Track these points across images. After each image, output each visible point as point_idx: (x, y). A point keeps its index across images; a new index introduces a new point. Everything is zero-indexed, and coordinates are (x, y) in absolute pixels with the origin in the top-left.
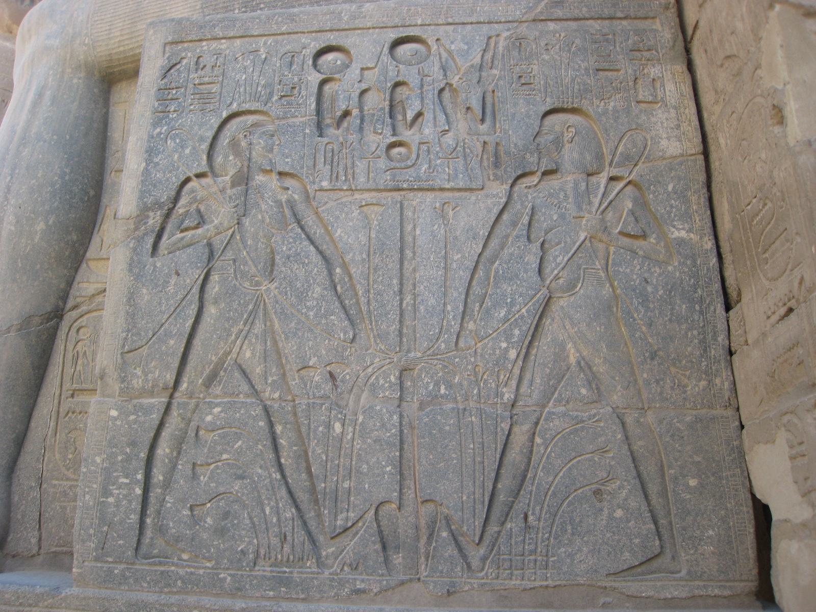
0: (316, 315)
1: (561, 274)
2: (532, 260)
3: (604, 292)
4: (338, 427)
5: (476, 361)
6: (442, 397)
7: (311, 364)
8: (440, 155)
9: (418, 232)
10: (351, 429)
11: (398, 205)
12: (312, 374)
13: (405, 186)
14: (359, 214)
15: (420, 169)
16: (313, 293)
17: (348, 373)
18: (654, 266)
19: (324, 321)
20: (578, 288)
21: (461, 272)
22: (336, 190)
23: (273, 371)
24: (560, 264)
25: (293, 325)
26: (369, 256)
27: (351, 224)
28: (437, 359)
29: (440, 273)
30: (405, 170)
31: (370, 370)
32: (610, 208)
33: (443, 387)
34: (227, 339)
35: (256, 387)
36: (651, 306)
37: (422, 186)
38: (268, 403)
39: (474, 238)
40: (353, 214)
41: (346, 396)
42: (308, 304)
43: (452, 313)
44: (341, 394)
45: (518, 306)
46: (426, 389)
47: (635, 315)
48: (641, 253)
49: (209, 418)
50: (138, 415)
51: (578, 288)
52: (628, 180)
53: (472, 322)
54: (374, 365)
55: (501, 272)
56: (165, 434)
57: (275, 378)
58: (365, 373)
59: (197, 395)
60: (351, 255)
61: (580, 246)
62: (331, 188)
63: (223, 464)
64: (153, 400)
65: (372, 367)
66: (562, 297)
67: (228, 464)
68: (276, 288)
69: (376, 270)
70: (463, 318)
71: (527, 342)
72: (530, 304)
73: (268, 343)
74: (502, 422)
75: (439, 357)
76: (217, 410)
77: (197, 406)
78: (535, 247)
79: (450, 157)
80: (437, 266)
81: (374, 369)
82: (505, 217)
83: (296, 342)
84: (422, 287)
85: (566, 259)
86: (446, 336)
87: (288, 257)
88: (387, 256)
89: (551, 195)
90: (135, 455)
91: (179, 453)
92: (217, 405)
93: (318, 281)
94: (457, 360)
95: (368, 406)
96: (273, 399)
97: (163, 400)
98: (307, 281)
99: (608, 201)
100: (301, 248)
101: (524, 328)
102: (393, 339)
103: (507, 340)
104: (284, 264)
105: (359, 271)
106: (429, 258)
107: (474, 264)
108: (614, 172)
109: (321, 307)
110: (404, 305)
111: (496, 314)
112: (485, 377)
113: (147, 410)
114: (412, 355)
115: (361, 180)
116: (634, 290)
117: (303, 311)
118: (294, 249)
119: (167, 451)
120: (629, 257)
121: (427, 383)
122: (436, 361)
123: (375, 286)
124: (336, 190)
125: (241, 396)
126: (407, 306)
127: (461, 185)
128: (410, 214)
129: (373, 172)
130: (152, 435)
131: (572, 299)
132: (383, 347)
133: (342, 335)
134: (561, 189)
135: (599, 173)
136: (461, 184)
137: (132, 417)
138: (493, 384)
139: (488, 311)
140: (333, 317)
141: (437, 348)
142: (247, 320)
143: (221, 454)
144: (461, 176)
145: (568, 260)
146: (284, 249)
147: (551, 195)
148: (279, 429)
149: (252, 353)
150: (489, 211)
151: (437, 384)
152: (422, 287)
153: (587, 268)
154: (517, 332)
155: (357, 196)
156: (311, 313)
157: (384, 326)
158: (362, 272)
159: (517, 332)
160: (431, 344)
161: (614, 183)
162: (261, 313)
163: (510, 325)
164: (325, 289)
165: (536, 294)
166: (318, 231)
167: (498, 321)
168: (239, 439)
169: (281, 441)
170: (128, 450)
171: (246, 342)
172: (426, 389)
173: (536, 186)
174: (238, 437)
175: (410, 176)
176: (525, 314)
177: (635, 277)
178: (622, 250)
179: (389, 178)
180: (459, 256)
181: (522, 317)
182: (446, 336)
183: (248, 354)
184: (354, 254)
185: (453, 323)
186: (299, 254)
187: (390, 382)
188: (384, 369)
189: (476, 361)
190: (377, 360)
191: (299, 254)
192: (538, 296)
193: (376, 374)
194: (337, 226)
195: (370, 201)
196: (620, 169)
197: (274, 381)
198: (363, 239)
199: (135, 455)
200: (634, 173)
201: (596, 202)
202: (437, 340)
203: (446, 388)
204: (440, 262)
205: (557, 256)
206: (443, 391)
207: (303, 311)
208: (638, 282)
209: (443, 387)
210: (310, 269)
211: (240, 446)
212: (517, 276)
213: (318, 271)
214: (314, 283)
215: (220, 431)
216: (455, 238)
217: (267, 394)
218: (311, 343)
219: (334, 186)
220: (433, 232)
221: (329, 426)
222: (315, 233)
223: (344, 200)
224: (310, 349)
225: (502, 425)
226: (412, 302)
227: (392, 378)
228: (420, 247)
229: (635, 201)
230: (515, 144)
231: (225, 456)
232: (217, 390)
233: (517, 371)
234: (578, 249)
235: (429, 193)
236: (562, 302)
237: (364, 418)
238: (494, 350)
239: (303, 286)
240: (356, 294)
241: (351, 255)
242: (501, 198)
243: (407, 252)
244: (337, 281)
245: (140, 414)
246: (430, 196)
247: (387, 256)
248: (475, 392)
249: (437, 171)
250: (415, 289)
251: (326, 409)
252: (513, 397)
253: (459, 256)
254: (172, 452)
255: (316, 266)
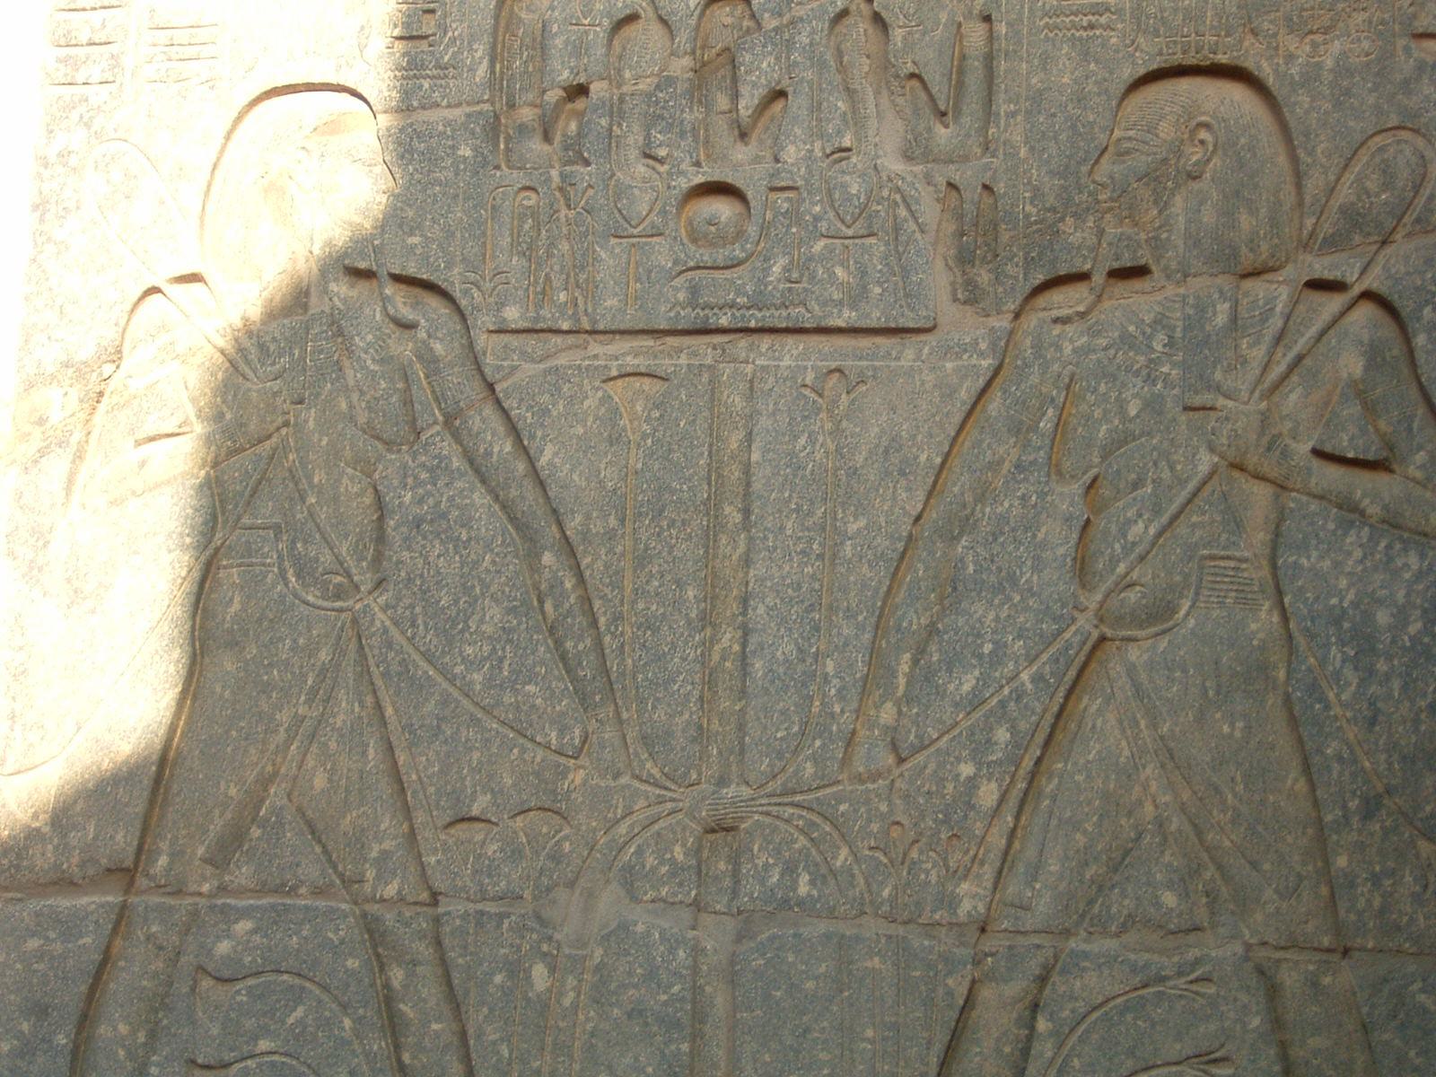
0: (489, 682)
1: (1135, 575)
2: (1058, 540)
3: (1254, 626)
4: (539, 972)
5: (891, 812)
6: (801, 903)
7: (475, 811)
8: (823, 226)
9: (755, 457)
10: (571, 981)
11: (705, 378)
12: (479, 837)
13: (724, 321)
14: (602, 401)
15: (767, 271)
16: (482, 621)
17: (566, 838)
18: (1405, 550)
19: (508, 699)
20: (1182, 612)
21: (865, 569)
22: (542, 331)
23: (383, 827)
24: (1134, 544)
25: (430, 707)
26: (622, 521)
27: (580, 430)
28: (797, 805)
29: (808, 570)
30: (728, 274)
31: (623, 829)
32: (1295, 378)
33: (804, 878)
34: (264, 742)
35: (340, 868)
36: (1382, 666)
37: (769, 323)
38: (374, 908)
39: (902, 473)
40: (586, 403)
41: (561, 894)
42: (469, 650)
43: (835, 681)
44: (549, 890)
45: (1011, 665)
46: (762, 882)
47: (1331, 695)
48: (1374, 510)
49: (224, 947)
50: (47, 938)
51: (1182, 612)
52: (1357, 290)
53: (889, 705)
54: (634, 817)
55: (971, 569)
56: (119, 984)
57: (387, 845)
58: (609, 837)
59: (193, 888)
60: (578, 518)
61: (1195, 494)
62: (526, 325)
63: (260, 1066)
64: (84, 900)
65: (628, 821)
66: (1135, 640)
67: (273, 1064)
68: (384, 609)
69: (641, 561)
70: (864, 693)
71: (1028, 763)
72: (1044, 657)
73: (371, 752)
74: (949, 973)
75: (798, 798)
76: (243, 926)
77: (195, 913)
78: (1067, 497)
79: (850, 232)
80: (803, 552)
81: (632, 826)
82: (995, 405)
83: (438, 753)
84: (761, 610)
85: (1152, 531)
86: (818, 743)
87: (418, 523)
88: (672, 524)
89: (1126, 340)
90: (43, 1040)
91: (152, 1035)
92: (245, 913)
93: (492, 589)
94: (843, 808)
95: (613, 925)
96: (383, 900)
97: (110, 899)
98: (467, 590)
99: (1291, 355)
100: (451, 499)
101: (1023, 726)
102: (683, 749)
103: (977, 755)
104: (407, 543)
105: (599, 565)
106: (782, 528)
107: (900, 546)
108: (1322, 267)
109: (501, 660)
110: (716, 657)
111: (951, 687)
112: (914, 854)
113: (69, 926)
114: (730, 792)
115: (608, 303)
116: (1337, 622)
117: (458, 670)
118: (431, 501)
119: (123, 1028)
120: (1331, 526)
121: (766, 866)
122: (791, 810)
123: (641, 606)
124: (542, 331)
125: (303, 890)
126: (723, 659)
127: (875, 318)
128: (738, 402)
129: (638, 280)
130: (84, 988)
131: (1163, 643)
132: (655, 771)
133: (554, 735)
134: (1159, 322)
135: (1273, 270)
136: (876, 314)
137: (33, 944)
138: (934, 872)
139: (929, 677)
140: (531, 688)
141: (796, 773)
142: (313, 692)
143: (255, 1039)
144: (878, 290)
145: (1159, 534)
146: (408, 497)
147: (1126, 340)
148: (397, 975)
149: (330, 780)
150: (950, 394)
151: (790, 870)
152: (761, 610)
153: (1213, 558)
154: (1002, 735)
155: (595, 348)
156: (477, 677)
157: (660, 715)
158: (607, 567)
159: (1002, 735)
160: (779, 764)
161: (1317, 297)
162: (349, 672)
163: (986, 717)
164: (511, 611)
165: (1060, 632)
166: (496, 449)
167: (956, 705)
168: (298, 1001)
169: (401, 1006)
170: (25, 1027)
171: (314, 748)
172: (762, 882)
173: (1082, 315)
174: (298, 996)
175: (738, 293)
176: (1029, 686)
177: (1343, 583)
178: (1314, 506)
179: (681, 296)
180: (862, 522)
181: (1019, 695)
182: (818, 743)
183: (320, 782)
184: (588, 517)
185: (837, 709)
186: (444, 516)
187: (673, 861)
188: (656, 827)
189: (891, 812)
190: (642, 803)
191: (444, 516)
192: (1067, 635)
193: (638, 841)
194: (544, 438)
195: (632, 362)
196: (1337, 258)
197: (385, 855)
198: (610, 476)
199: (43, 1040)
200: (1377, 270)
201: (1258, 354)
202: (796, 752)
203: (812, 883)
204: (810, 541)
205: (1130, 522)
206: (803, 889)
207: (458, 670)
208: (1351, 596)
209: (804, 878)
210: (473, 556)
211: (300, 1022)
212: (1013, 579)
213: (494, 562)
214: (483, 594)
215: (251, 982)
216: (853, 472)
217: (368, 888)
218: (476, 755)
219: (537, 319)
220: (792, 454)
221: (517, 970)
222: (488, 454)
223: (562, 361)
224: (472, 770)
225: (950, 982)
226: (736, 648)
227: (678, 853)
228: (760, 497)
229: (1374, 355)
230: (1036, 189)
231: (264, 1045)
232: (243, 874)
233: (997, 840)
234: (1189, 501)
235: (790, 340)
236: (1134, 654)
237: (606, 954)
238: (941, 781)
239: (456, 602)
240: (594, 623)
241: (578, 518)
242: (982, 355)
243: (728, 510)
244: (543, 587)
245: (52, 935)
246: (791, 351)
247: (672, 524)
248: (886, 893)
249: (813, 277)
250: (744, 614)
251: (511, 929)
252: (981, 908)
253: (862, 522)
254: (134, 1032)
255: (488, 547)
